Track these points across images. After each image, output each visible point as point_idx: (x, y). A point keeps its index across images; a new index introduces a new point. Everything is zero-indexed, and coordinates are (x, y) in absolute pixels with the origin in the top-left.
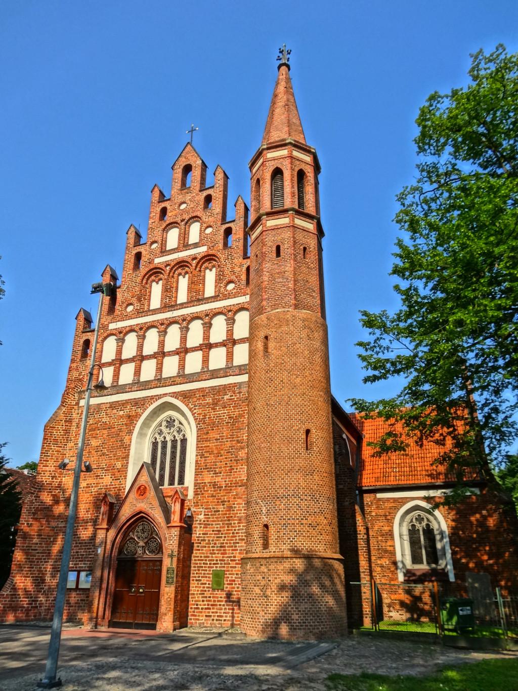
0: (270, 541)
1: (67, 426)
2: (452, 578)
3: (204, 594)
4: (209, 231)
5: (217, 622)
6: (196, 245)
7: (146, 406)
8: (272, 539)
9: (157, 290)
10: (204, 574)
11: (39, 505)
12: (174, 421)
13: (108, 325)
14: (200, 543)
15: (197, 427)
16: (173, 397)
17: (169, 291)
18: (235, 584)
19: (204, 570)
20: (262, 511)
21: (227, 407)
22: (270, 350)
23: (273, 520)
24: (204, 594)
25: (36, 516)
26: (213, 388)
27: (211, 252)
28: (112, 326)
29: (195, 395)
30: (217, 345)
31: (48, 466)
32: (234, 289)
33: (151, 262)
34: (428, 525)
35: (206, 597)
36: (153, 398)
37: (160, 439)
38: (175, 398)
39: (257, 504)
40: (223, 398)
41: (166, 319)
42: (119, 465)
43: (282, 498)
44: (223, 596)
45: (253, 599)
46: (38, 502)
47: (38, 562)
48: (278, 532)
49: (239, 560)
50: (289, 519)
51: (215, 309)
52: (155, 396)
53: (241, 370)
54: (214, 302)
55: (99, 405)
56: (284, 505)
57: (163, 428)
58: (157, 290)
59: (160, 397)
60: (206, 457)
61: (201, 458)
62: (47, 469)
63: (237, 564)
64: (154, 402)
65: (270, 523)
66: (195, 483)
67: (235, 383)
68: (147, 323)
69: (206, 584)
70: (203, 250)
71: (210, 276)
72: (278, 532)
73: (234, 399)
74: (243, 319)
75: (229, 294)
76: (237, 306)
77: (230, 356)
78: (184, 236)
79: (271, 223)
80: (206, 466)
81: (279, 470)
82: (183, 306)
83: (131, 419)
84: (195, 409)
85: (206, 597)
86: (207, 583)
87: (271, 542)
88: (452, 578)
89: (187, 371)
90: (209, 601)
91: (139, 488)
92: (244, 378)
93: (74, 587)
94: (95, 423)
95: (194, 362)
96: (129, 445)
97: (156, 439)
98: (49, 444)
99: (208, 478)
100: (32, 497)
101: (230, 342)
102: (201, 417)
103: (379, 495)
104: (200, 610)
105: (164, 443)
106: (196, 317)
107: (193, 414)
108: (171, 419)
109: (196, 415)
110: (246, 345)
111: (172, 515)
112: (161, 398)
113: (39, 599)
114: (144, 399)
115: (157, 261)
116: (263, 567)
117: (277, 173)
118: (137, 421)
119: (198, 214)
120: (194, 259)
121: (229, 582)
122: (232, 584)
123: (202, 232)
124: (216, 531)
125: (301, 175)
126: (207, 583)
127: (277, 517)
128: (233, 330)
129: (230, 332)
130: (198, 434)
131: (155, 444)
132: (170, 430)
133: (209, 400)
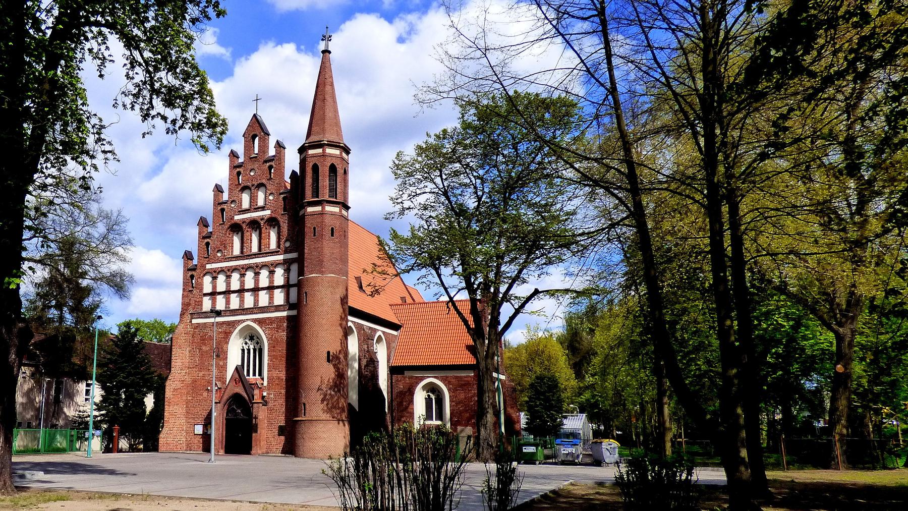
4: (271, 198)
6: (263, 208)
27: (274, 215)
28: (208, 266)
33: (232, 218)
37: (246, 347)
42: (221, 363)
58: (236, 241)
59: (244, 321)
70: (268, 212)
74: (294, 268)
78: (253, 199)
79: (310, 209)
82: (255, 255)
83: (227, 335)
89: (261, 305)
95: (264, 299)
99: (275, 373)
101: (286, 287)
105: (249, 350)
106: (264, 266)
115: (237, 218)
117: (315, 168)
119: (264, 181)
120: (262, 219)
125: (333, 169)
131: (243, 350)
133: (274, 326)
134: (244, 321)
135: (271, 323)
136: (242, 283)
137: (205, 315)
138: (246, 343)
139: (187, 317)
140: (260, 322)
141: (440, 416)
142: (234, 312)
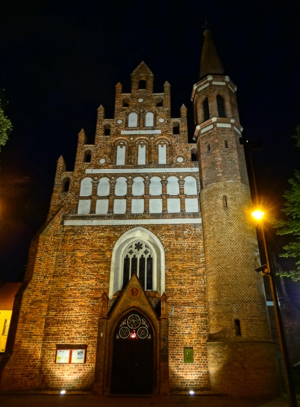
0: (241, 330)
1: (55, 239)
3: (178, 367)
5: (190, 386)
6: (153, 129)
7: (123, 232)
8: (243, 330)
9: (121, 152)
10: (178, 352)
11: (35, 298)
12: (142, 245)
13: (85, 170)
14: (173, 331)
15: (164, 250)
16: (144, 228)
18: (202, 360)
19: (177, 350)
20: (232, 310)
21: (186, 239)
22: (228, 206)
23: (242, 317)
24: (178, 367)
25: (32, 307)
26: (175, 226)
28: (88, 171)
29: (161, 228)
30: (173, 197)
31: (41, 268)
32: (183, 162)
35: (180, 369)
36: (129, 227)
37: (131, 257)
38: (146, 229)
39: (228, 306)
40: (183, 233)
41: (133, 173)
43: (247, 302)
44: (193, 368)
45: (233, 370)
46: (34, 295)
47: (33, 342)
48: (247, 325)
49: (203, 343)
50: (253, 317)
51: (170, 173)
52: (129, 225)
53: (194, 215)
54: (169, 168)
55: (82, 227)
56: (249, 307)
57: (133, 249)
58: (121, 152)
59: (133, 226)
60: (173, 271)
61: (169, 271)
62: (41, 270)
63: (202, 345)
64: (129, 229)
65: (241, 319)
66: (165, 289)
67: (191, 224)
68: (118, 173)
69: (179, 360)
71: (162, 151)
72: (247, 325)
73: (191, 234)
75: (180, 165)
76: (186, 173)
77: (183, 204)
79: (219, 125)
80: (173, 277)
81: (243, 284)
83: (111, 240)
84: (162, 238)
85: (180, 369)
86: (180, 359)
87: (242, 331)
90: (183, 372)
91: (132, 290)
92: (198, 221)
93: (67, 361)
94: (79, 240)
96: (111, 258)
97: (127, 256)
98: (42, 251)
100: (29, 291)
102: (167, 244)
104: (176, 378)
105: (134, 259)
107: (161, 241)
108: (139, 243)
109: (163, 242)
110: (196, 201)
111: (162, 311)
112: (134, 227)
113: (35, 372)
114: (121, 226)
116: (240, 348)
118: (116, 242)
121: (197, 358)
122: (199, 360)
124: (184, 323)
126: (180, 359)
127: (245, 315)
128: (183, 188)
130: (165, 255)
131: (127, 260)
132: (138, 250)
133: (173, 233)
135: (168, 230)
137: (83, 217)
138: (131, 252)
139: (57, 220)
140: (154, 229)
142: (120, 217)
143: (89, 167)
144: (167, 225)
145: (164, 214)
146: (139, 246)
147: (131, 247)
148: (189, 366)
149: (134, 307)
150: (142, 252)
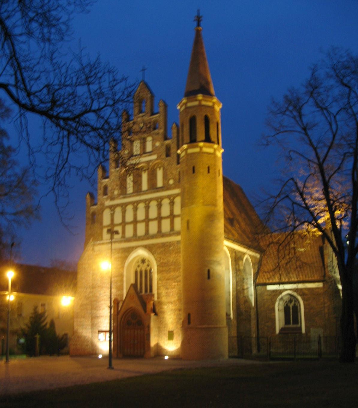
2: (303, 331)
4: (158, 144)
6: (151, 153)
17: (137, 183)
34: (295, 305)
37: (139, 270)
71: (160, 174)
74: (178, 200)
82: (146, 193)
88: (303, 331)
97: (137, 269)
103: (270, 288)
105: (141, 272)
123: (153, 145)
129: (172, 211)
131: (136, 273)
134: (136, 248)
136: (135, 216)
138: (139, 266)
141: (296, 320)
143: (107, 199)
144: (158, 244)
145: (160, 234)
146: (143, 261)
147: (138, 262)
148: (171, 342)
149: (131, 308)
150: (146, 264)
